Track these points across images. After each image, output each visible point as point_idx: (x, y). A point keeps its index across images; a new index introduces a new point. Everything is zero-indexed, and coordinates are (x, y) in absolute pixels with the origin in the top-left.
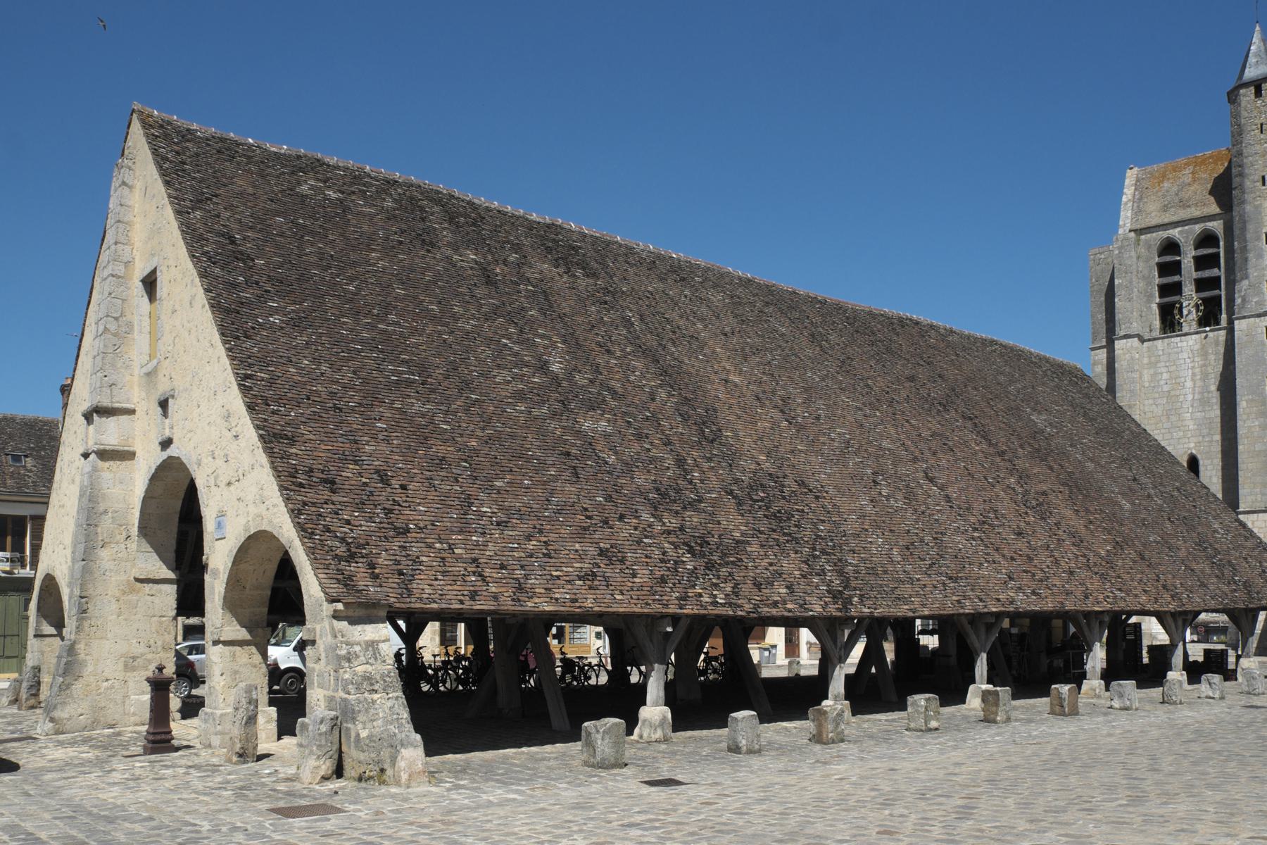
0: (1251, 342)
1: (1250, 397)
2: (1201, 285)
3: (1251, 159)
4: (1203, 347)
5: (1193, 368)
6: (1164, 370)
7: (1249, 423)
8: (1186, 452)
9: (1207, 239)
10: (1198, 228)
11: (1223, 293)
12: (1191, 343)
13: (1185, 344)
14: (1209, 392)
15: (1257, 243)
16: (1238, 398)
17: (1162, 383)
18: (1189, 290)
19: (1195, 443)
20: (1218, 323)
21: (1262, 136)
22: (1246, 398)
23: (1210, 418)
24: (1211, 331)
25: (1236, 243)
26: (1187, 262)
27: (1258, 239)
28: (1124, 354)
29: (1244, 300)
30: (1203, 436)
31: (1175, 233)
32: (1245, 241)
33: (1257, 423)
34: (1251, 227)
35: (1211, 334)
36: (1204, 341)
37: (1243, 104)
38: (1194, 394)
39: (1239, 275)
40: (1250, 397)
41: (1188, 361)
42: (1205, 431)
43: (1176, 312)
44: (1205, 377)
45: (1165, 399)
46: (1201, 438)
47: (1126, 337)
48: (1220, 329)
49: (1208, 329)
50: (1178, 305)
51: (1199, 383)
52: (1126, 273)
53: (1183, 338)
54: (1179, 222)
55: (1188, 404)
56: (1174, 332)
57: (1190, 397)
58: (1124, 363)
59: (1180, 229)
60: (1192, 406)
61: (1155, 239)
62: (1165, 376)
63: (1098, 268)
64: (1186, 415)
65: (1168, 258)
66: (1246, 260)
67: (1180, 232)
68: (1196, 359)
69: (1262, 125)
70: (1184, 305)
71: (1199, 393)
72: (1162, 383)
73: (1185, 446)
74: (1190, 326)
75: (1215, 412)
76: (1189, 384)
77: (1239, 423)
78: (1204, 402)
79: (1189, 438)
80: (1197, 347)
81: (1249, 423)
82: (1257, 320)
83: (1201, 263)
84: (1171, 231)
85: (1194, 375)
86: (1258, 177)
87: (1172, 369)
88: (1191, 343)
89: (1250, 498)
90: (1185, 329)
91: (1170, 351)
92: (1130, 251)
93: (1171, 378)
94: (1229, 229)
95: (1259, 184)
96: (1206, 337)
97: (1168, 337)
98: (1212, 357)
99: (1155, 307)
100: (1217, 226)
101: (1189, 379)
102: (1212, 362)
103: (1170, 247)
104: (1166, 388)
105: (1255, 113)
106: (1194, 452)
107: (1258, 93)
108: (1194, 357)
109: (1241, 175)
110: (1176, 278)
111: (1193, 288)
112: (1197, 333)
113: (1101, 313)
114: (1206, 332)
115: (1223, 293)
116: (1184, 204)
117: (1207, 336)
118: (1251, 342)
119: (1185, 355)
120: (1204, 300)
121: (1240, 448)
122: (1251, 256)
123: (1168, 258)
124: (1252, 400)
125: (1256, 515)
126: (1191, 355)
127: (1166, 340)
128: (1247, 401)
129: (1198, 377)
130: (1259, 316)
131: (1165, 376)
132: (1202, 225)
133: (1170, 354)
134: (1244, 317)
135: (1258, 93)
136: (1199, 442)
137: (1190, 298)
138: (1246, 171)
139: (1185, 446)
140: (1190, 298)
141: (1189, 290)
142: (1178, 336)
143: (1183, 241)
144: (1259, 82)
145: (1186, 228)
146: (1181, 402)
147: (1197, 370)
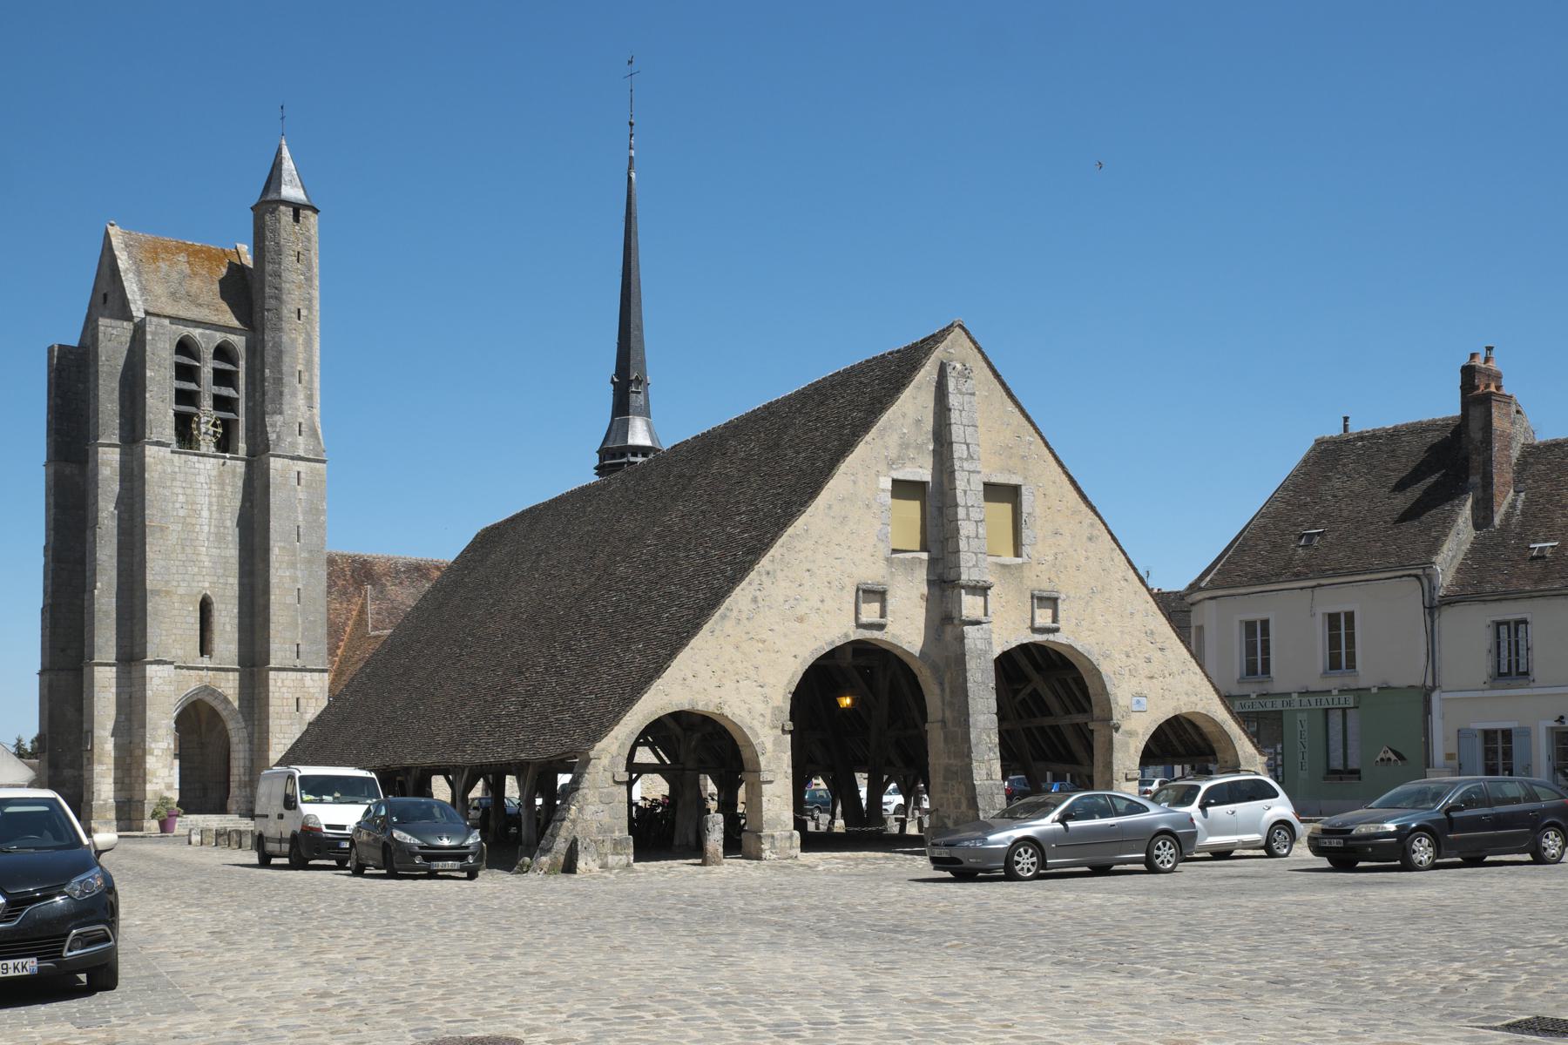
0: (285, 485)
1: (282, 544)
2: (221, 403)
3: (288, 285)
4: (221, 474)
5: (210, 495)
6: (180, 491)
7: (280, 573)
8: (200, 592)
9: (223, 352)
10: (219, 337)
11: (242, 419)
12: (208, 466)
13: (202, 466)
14: (225, 527)
15: (291, 379)
16: (272, 543)
17: (178, 505)
18: (207, 404)
19: (210, 583)
20: (236, 452)
21: (299, 266)
22: (279, 544)
23: (225, 557)
24: (231, 458)
25: (267, 371)
26: (207, 367)
27: (293, 375)
28: (156, 464)
29: (278, 437)
30: (218, 577)
31: (196, 333)
32: (280, 372)
33: (288, 574)
34: (286, 359)
35: (228, 462)
36: (222, 468)
37: (283, 222)
38: (210, 526)
39: (269, 407)
40: (282, 544)
41: (205, 486)
42: (220, 571)
43: (194, 426)
44: (221, 510)
45: (180, 525)
46: (216, 578)
47: (159, 444)
48: (237, 459)
49: (228, 455)
50: (195, 419)
51: (215, 515)
52: (160, 366)
53: (200, 458)
54: (192, 321)
55: (203, 537)
56: (191, 448)
57: (206, 529)
58: (156, 475)
59: (200, 330)
60: (208, 539)
61: (174, 333)
62: (181, 498)
63: (109, 344)
64: (201, 549)
65: (186, 360)
66: (281, 394)
67: (201, 334)
68: (214, 487)
69: (299, 253)
70: (202, 421)
71: (215, 526)
72: (178, 505)
73: (200, 584)
74: (208, 446)
75: (232, 552)
76: (205, 513)
77: (272, 571)
78: (220, 538)
79: (204, 576)
80: (214, 473)
81: (280, 573)
82: (291, 462)
83: (222, 378)
84: (191, 330)
85: (210, 504)
86: (294, 308)
87: (189, 491)
88: (208, 466)
89: (280, 654)
90: (203, 450)
91: (187, 470)
92: (165, 342)
93: (187, 502)
94: (255, 350)
95: (295, 316)
96: (224, 464)
97: (185, 453)
98: (229, 489)
99: (171, 413)
100: (239, 342)
101: (205, 507)
102: (229, 494)
103: (184, 347)
104: (182, 513)
105: (292, 238)
106: (208, 593)
107: (296, 218)
108: (211, 484)
109: (278, 298)
110: (193, 386)
111: (211, 403)
112: (215, 457)
113: (111, 402)
114: (224, 457)
115: (242, 419)
116: (194, 300)
117: (224, 464)
118: (285, 485)
119: (202, 479)
120: (221, 419)
121: (272, 597)
122: (286, 390)
123: (186, 360)
124: (284, 548)
125: (285, 673)
126: (208, 481)
127: (183, 456)
128: (279, 548)
129: (215, 508)
130: (292, 458)
131: (181, 498)
132: (223, 335)
133: (186, 473)
134: (279, 456)
135: (296, 218)
136: (215, 583)
137: (207, 415)
138: (284, 297)
139: (200, 584)
140: (207, 415)
141: (207, 404)
142: (195, 455)
143: (203, 346)
144: (296, 206)
145: (207, 332)
146: (197, 532)
147: (214, 500)
